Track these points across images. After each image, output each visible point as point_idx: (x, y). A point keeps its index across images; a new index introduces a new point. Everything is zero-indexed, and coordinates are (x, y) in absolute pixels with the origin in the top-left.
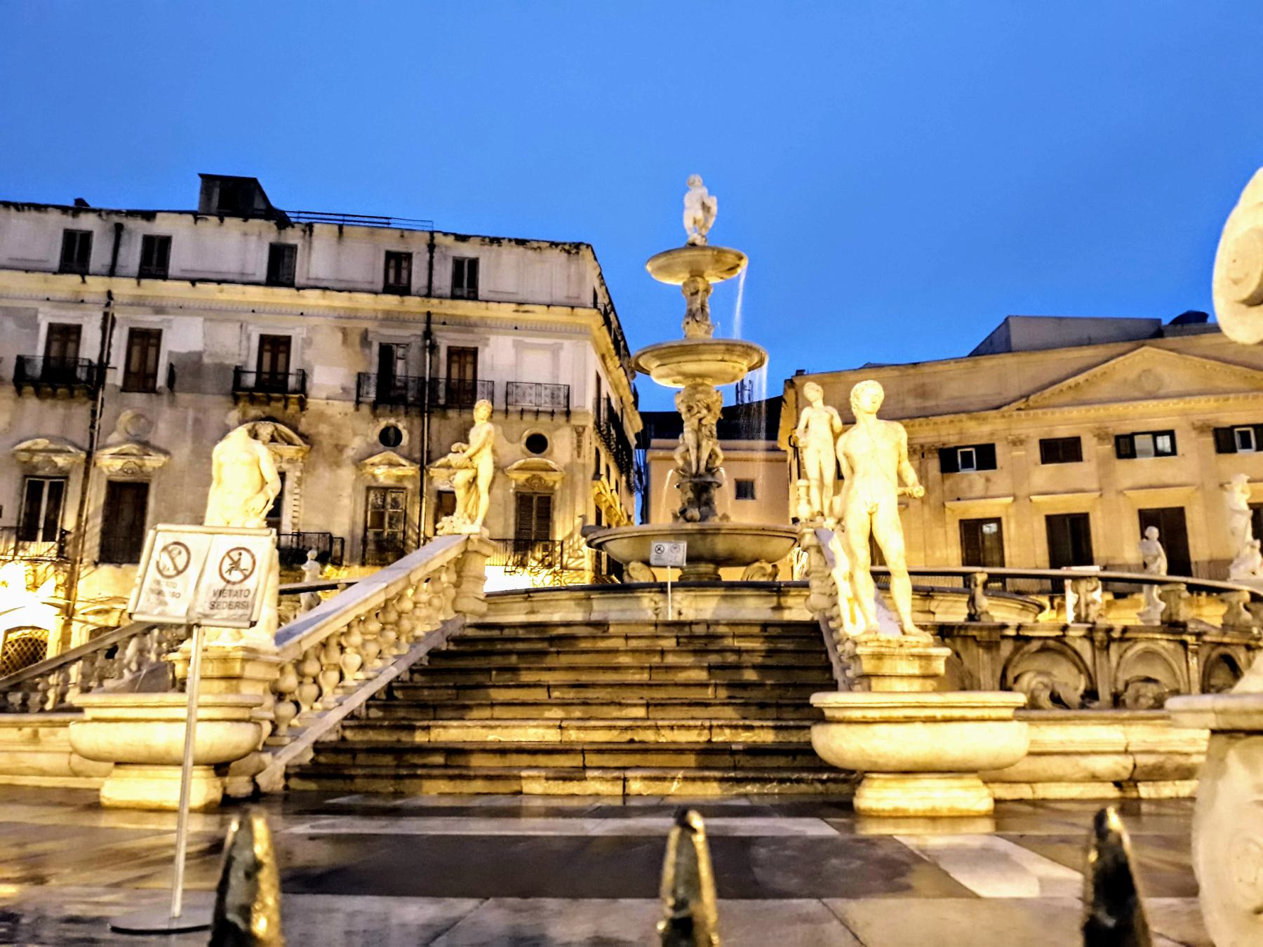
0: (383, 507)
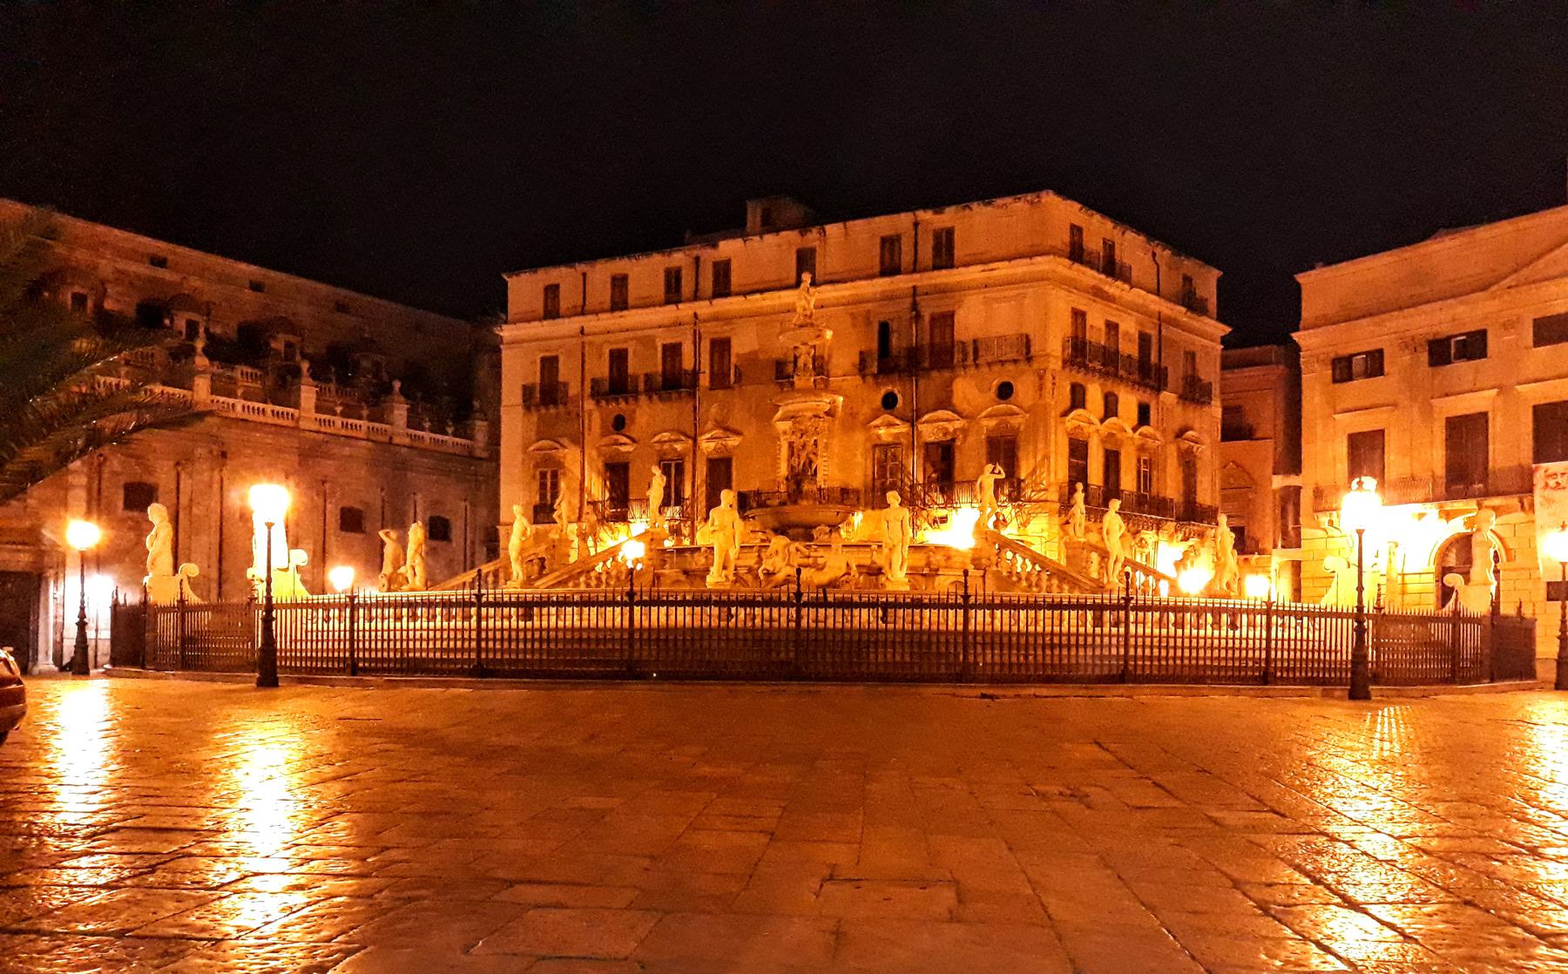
0: (886, 461)
